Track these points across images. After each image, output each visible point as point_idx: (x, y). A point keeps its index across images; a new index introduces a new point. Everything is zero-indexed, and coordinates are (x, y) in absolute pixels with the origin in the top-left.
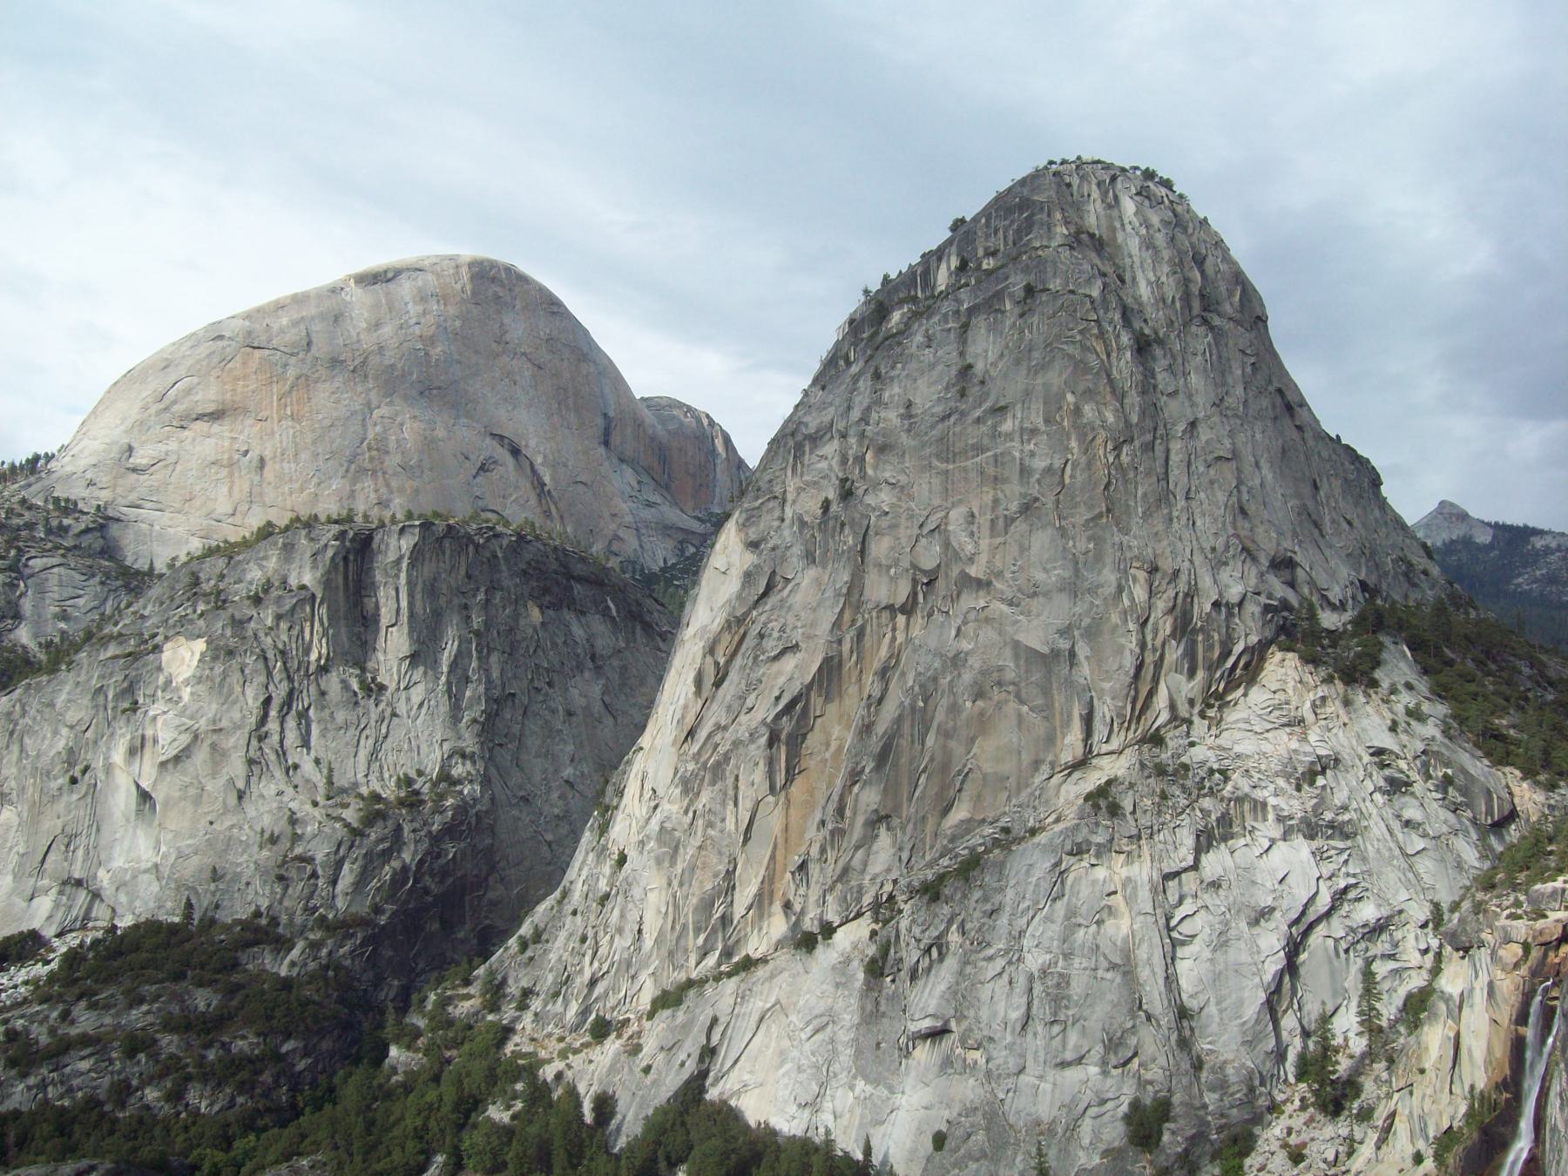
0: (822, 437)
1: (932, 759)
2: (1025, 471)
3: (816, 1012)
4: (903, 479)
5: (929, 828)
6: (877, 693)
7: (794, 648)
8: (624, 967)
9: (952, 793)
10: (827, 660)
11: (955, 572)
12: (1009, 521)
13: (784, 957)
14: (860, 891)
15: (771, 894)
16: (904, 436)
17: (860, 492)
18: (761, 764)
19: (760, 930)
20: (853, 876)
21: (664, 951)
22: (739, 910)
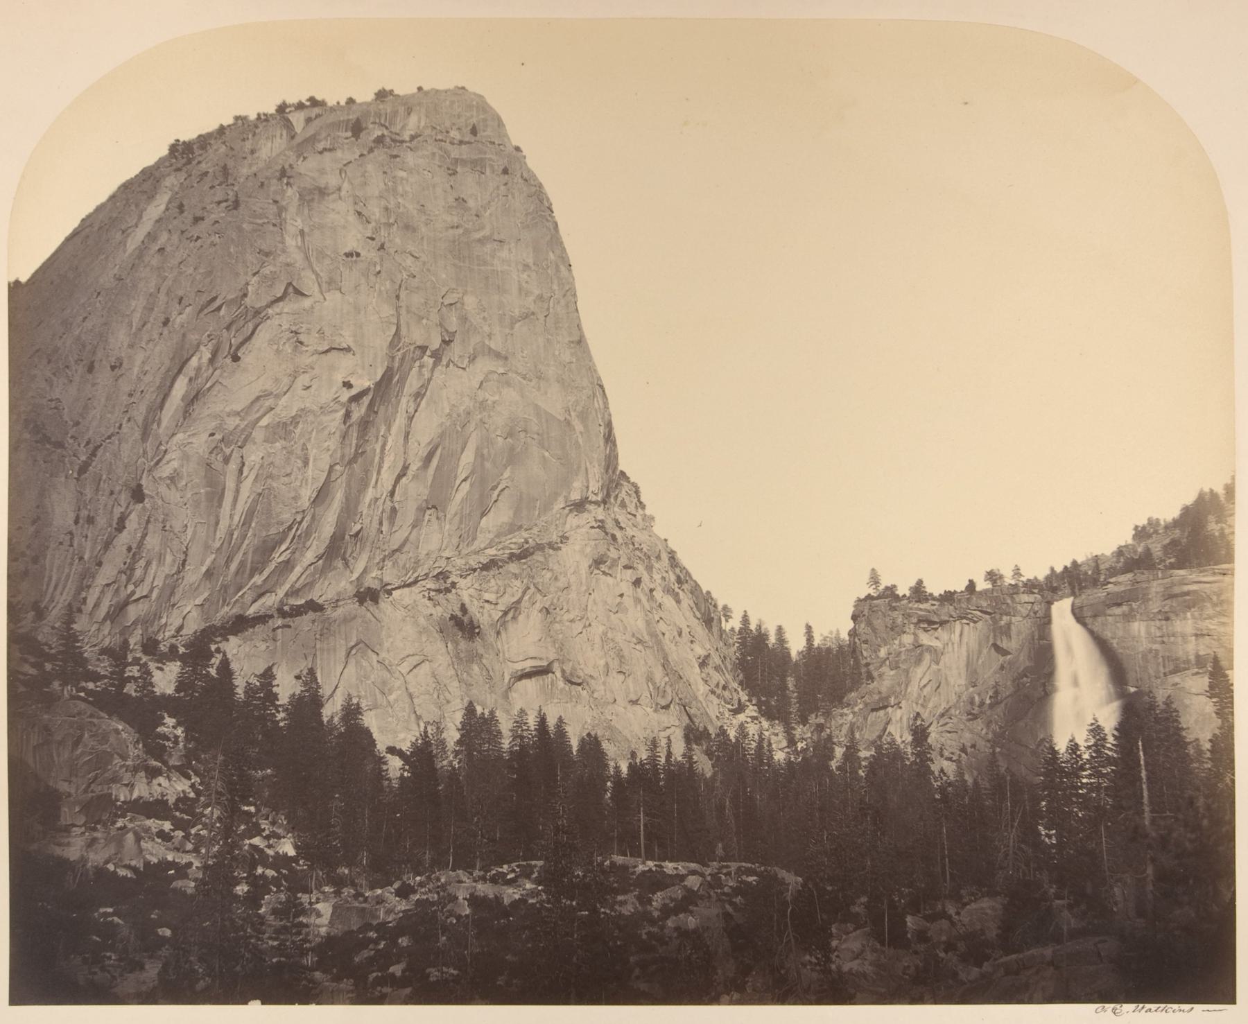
11: (475, 340)
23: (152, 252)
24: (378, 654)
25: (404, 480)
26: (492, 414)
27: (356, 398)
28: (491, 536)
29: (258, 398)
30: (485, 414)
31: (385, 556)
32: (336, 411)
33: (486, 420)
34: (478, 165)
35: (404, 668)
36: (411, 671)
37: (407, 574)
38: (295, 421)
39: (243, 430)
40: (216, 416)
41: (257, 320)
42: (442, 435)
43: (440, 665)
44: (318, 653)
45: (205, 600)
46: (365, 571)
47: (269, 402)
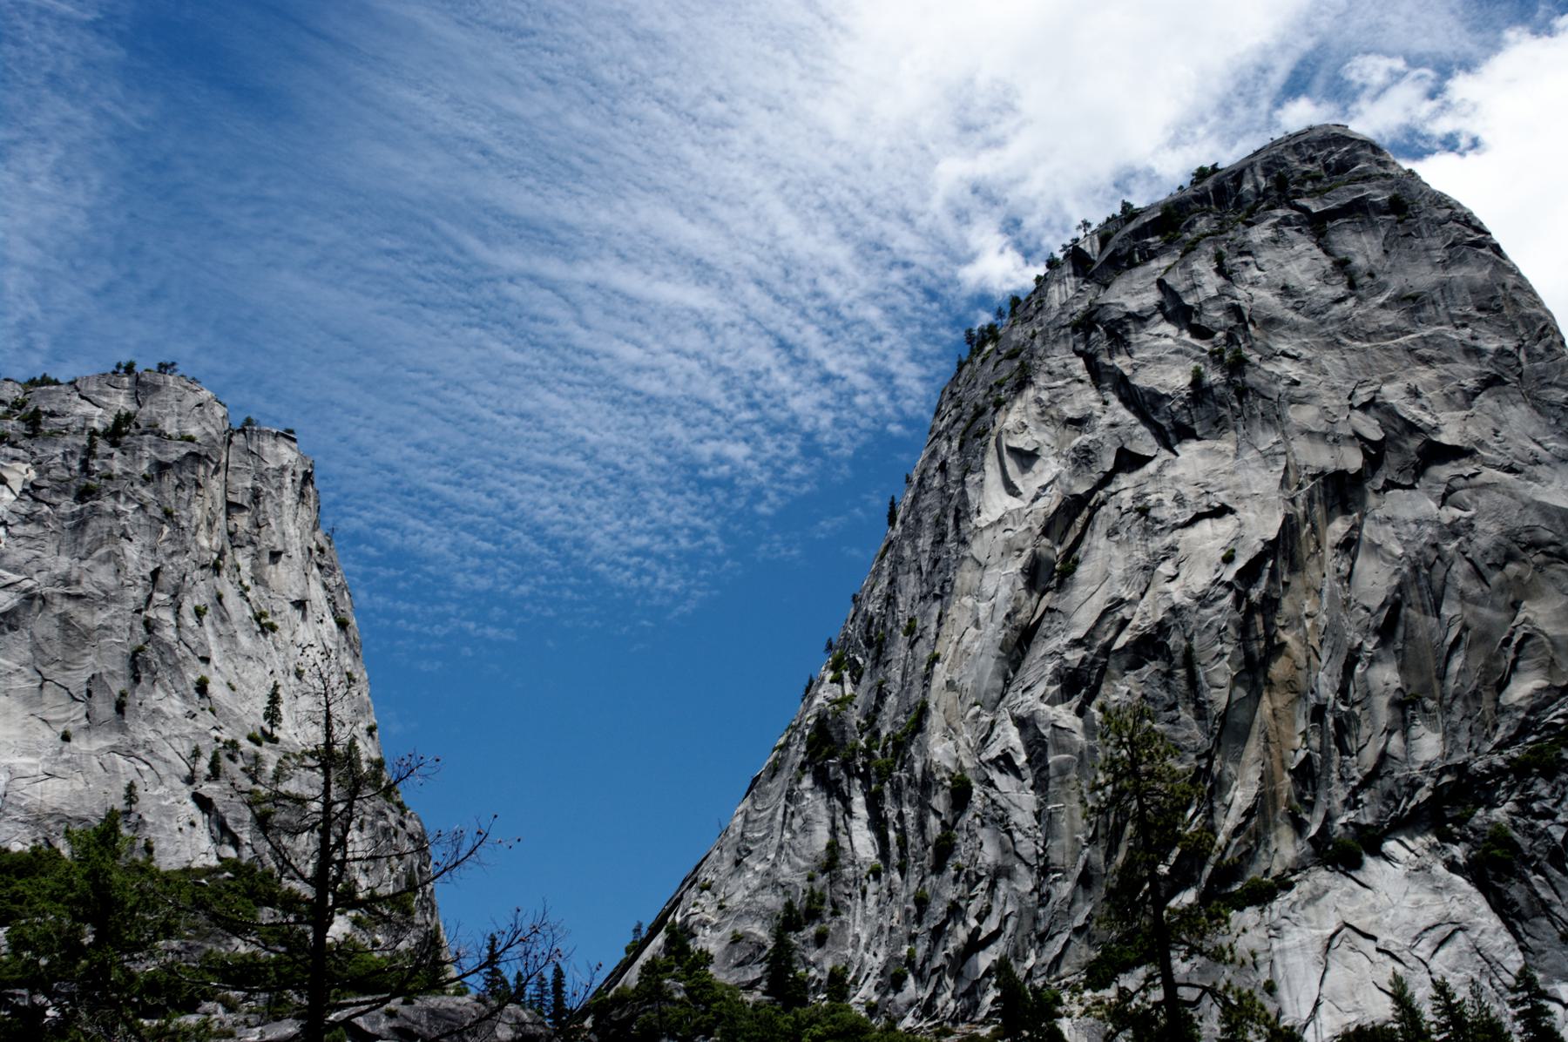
0: (1146, 319)
1: (1465, 628)
2: (1473, 352)
3: (1422, 925)
4: (1306, 354)
5: (1487, 704)
6: (1344, 567)
7: (1221, 512)
8: (1027, 921)
9: (1505, 664)
10: (1288, 519)
11: (1414, 443)
12: (1471, 396)
13: (1322, 876)
14: (1414, 786)
15: (1274, 795)
16: (1291, 314)
17: (1255, 358)
18: (1231, 630)
19: (1268, 843)
20: (1390, 765)
21: (1099, 893)
22: (1228, 822)
23: (931, 472)
24: (1374, 938)
25: (1359, 669)
26: (1472, 535)
27: (1249, 574)
28: (1521, 715)
29: (1105, 614)
30: (1461, 539)
31: (1354, 788)
32: (1222, 597)
33: (1466, 547)
34: (1358, 211)
35: (1424, 950)
36: (1435, 951)
37: (1397, 807)
38: (1162, 628)
39: (1094, 662)
40: (1051, 655)
41: (1086, 513)
42: (1399, 588)
43: (1483, 932)
44: (1277, 958)
45: (1087, 918)
46: (1329, 818)
47: (1126, 612)
